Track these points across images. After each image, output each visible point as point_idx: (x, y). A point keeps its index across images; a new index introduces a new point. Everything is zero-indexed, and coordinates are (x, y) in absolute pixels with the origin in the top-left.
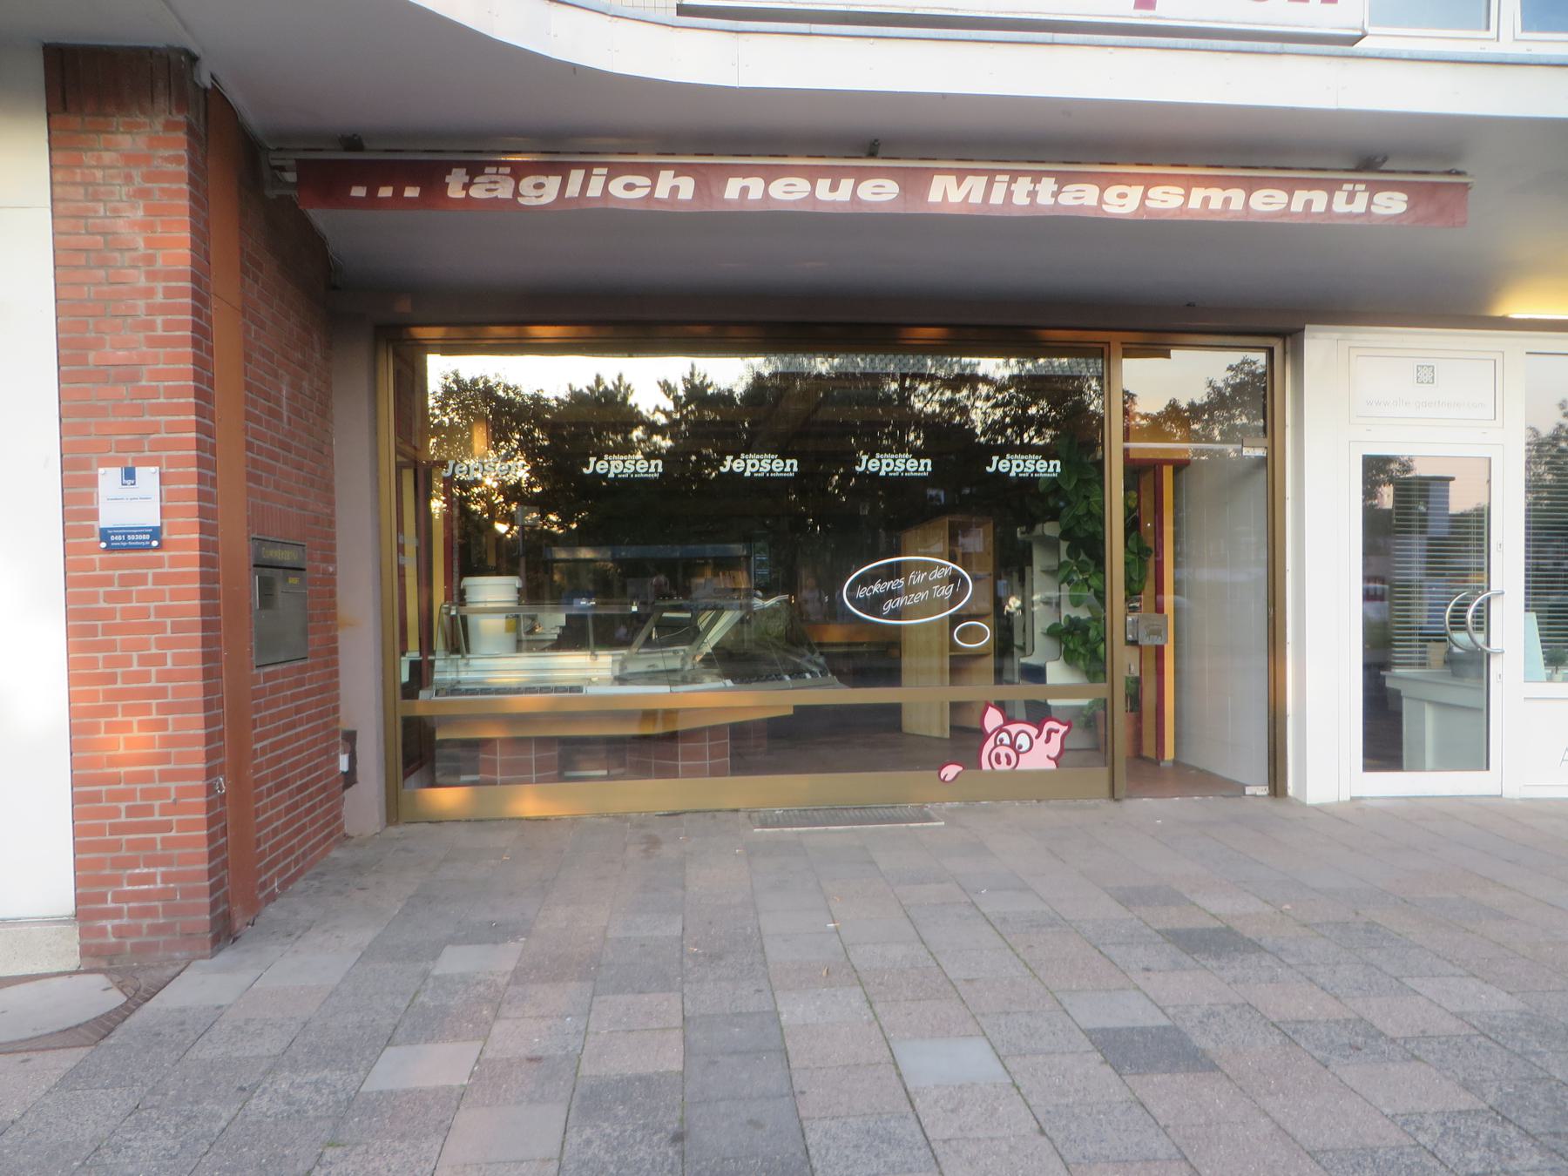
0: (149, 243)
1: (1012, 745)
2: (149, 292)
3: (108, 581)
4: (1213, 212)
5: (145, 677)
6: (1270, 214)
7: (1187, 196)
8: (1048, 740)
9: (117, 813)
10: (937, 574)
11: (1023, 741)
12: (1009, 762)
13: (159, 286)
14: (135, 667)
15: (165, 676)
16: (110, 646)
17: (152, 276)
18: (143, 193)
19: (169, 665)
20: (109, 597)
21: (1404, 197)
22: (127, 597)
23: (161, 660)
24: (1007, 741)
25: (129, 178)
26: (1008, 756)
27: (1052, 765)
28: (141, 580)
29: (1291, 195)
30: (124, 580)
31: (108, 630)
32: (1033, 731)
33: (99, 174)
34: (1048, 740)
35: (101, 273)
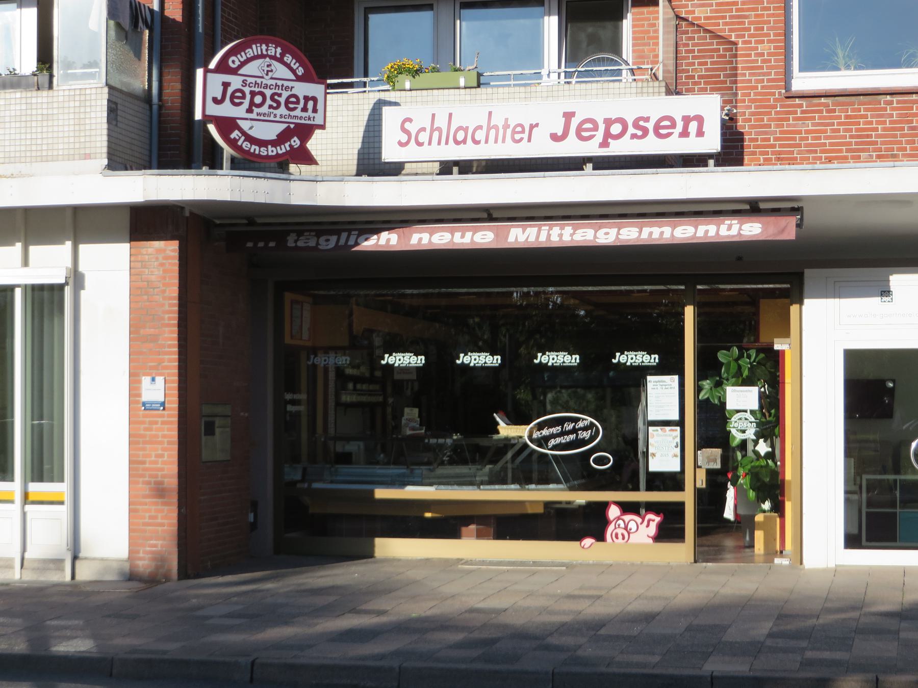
0: (164, 285)
1: (626, 528)
2: (163, 305)
3: (143, 423)
4: (654, 239)
5: (156, 463)
6: (684, 238)
7: (640, 232)
8: (648, 526)
9: (144, 518)
10: (581, 424)
11: (632, 526)
12: (623, 538)
13: (167, 302)
14: (153, 458)
15: (164, 463)
16: (144, 449)
17: (164, 298)
18: (162, 265)
19: (166, 458)
20: (146, 429)
21: (760, 225)
22: (150, 429)
23: (162, 456)
24: (622, 525)
25: (157, 259)
26: (623, 535)
27: (651, 541)
28: (156, 423)
29: (696, 228)
30: (151, 423)
31: (145, 443)
32: (639, 520)
33: (147, 257)
34: (648, 526)
35: (146, 297)
